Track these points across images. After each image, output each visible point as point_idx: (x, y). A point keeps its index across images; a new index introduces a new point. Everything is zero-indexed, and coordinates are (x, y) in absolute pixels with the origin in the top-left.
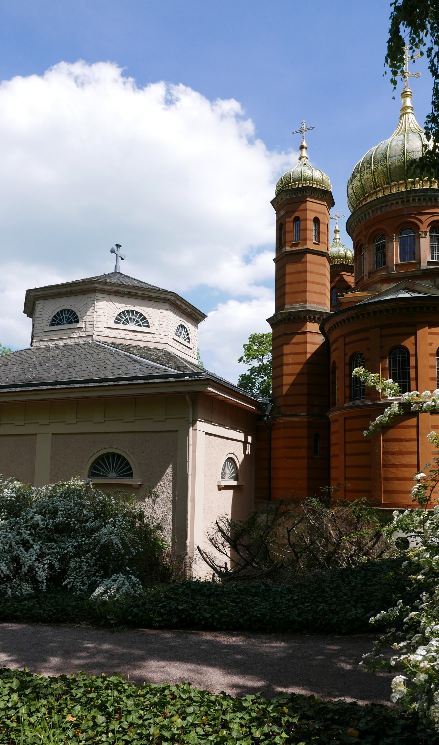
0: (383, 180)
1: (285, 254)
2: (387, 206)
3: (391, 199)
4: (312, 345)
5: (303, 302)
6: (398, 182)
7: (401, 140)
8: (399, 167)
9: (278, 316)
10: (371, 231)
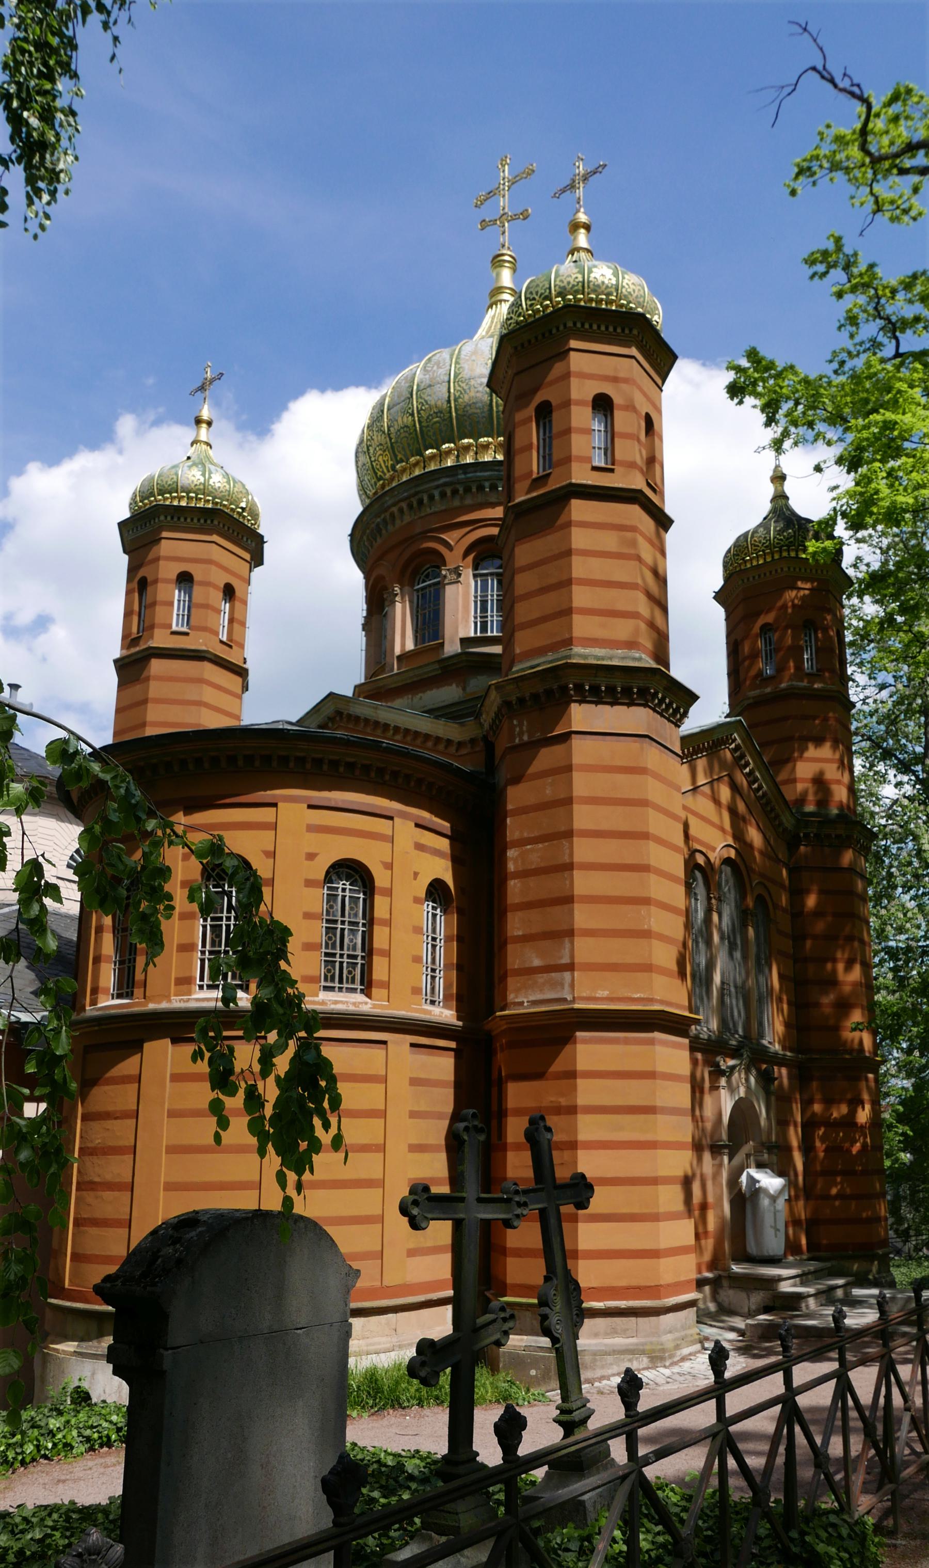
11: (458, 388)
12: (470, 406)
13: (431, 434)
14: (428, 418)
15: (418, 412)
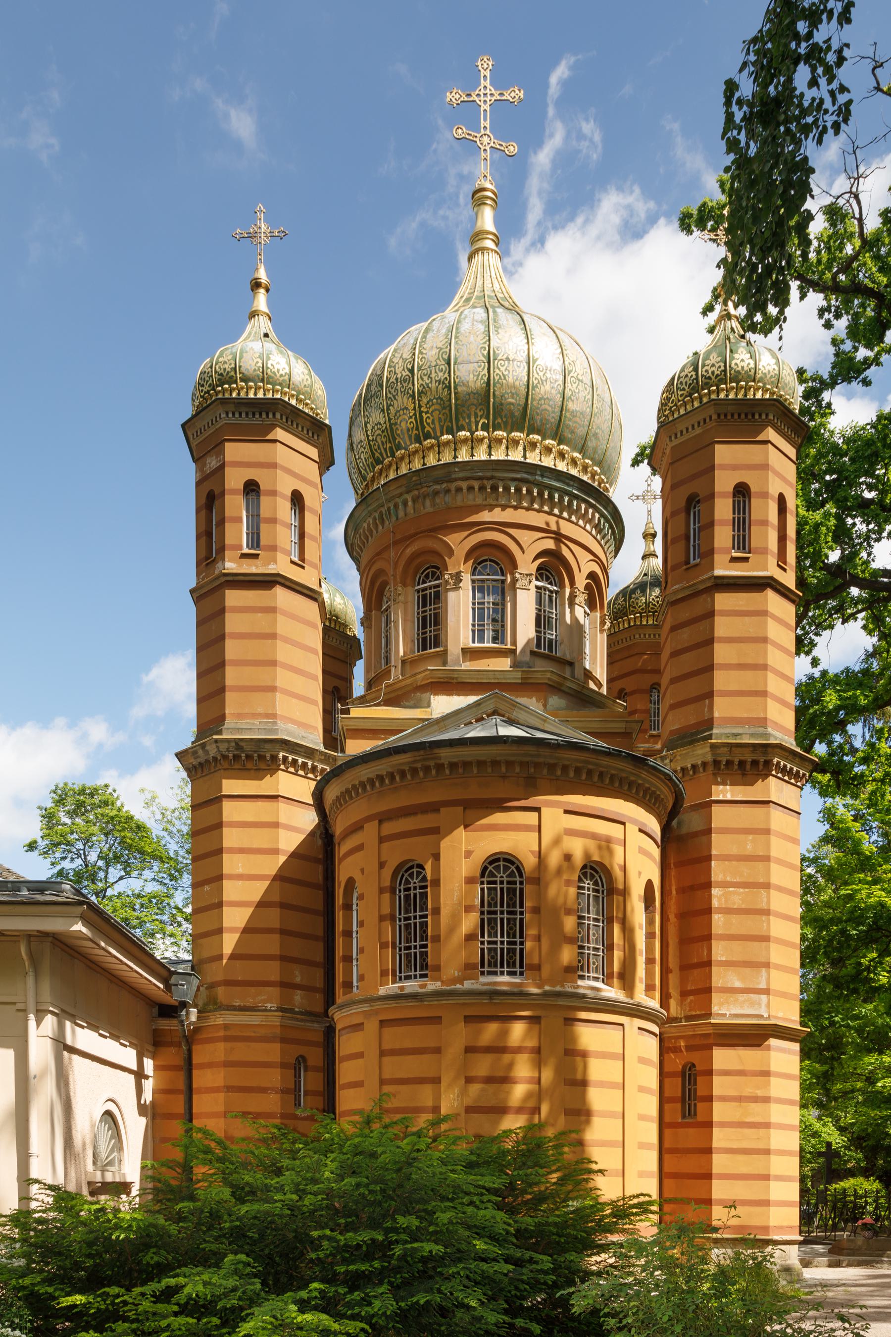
1: (223, 579)
4: (290, 833)
5: (267, 716)
7: (481, 322)
8: (475, 393)
9: (208, 748)
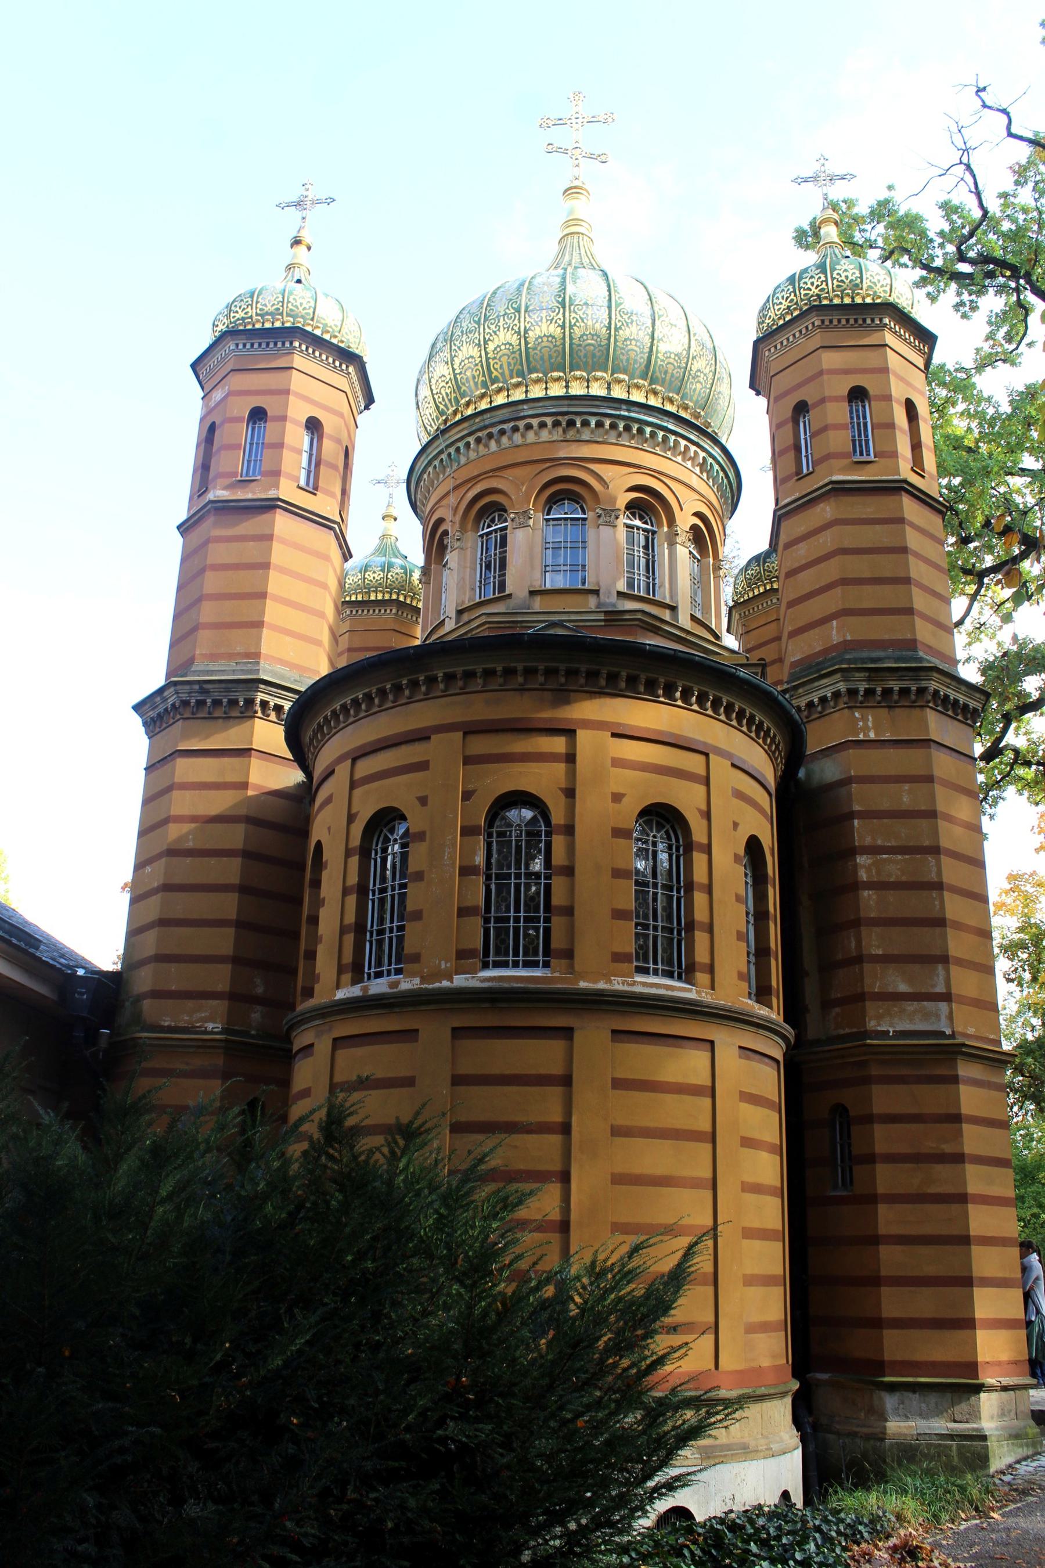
0: (509, 364)
2: (515, 429)
3: (526, 413)
6: (545, 375)
10: (471, 495)
11: (619, 318)
12: (631, 340)
13: (582, 354)
14: (582, 336)
15: (571, 327)
